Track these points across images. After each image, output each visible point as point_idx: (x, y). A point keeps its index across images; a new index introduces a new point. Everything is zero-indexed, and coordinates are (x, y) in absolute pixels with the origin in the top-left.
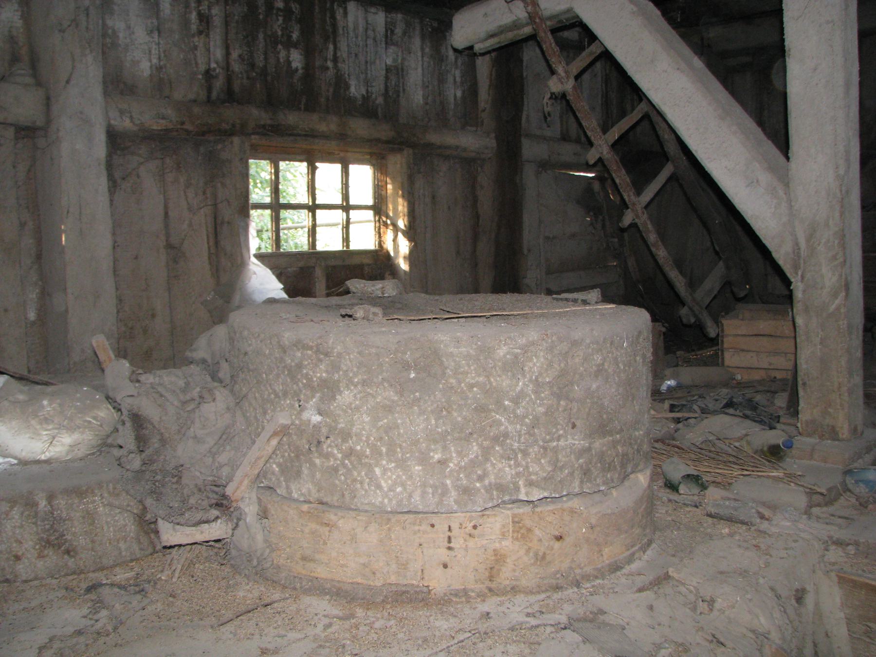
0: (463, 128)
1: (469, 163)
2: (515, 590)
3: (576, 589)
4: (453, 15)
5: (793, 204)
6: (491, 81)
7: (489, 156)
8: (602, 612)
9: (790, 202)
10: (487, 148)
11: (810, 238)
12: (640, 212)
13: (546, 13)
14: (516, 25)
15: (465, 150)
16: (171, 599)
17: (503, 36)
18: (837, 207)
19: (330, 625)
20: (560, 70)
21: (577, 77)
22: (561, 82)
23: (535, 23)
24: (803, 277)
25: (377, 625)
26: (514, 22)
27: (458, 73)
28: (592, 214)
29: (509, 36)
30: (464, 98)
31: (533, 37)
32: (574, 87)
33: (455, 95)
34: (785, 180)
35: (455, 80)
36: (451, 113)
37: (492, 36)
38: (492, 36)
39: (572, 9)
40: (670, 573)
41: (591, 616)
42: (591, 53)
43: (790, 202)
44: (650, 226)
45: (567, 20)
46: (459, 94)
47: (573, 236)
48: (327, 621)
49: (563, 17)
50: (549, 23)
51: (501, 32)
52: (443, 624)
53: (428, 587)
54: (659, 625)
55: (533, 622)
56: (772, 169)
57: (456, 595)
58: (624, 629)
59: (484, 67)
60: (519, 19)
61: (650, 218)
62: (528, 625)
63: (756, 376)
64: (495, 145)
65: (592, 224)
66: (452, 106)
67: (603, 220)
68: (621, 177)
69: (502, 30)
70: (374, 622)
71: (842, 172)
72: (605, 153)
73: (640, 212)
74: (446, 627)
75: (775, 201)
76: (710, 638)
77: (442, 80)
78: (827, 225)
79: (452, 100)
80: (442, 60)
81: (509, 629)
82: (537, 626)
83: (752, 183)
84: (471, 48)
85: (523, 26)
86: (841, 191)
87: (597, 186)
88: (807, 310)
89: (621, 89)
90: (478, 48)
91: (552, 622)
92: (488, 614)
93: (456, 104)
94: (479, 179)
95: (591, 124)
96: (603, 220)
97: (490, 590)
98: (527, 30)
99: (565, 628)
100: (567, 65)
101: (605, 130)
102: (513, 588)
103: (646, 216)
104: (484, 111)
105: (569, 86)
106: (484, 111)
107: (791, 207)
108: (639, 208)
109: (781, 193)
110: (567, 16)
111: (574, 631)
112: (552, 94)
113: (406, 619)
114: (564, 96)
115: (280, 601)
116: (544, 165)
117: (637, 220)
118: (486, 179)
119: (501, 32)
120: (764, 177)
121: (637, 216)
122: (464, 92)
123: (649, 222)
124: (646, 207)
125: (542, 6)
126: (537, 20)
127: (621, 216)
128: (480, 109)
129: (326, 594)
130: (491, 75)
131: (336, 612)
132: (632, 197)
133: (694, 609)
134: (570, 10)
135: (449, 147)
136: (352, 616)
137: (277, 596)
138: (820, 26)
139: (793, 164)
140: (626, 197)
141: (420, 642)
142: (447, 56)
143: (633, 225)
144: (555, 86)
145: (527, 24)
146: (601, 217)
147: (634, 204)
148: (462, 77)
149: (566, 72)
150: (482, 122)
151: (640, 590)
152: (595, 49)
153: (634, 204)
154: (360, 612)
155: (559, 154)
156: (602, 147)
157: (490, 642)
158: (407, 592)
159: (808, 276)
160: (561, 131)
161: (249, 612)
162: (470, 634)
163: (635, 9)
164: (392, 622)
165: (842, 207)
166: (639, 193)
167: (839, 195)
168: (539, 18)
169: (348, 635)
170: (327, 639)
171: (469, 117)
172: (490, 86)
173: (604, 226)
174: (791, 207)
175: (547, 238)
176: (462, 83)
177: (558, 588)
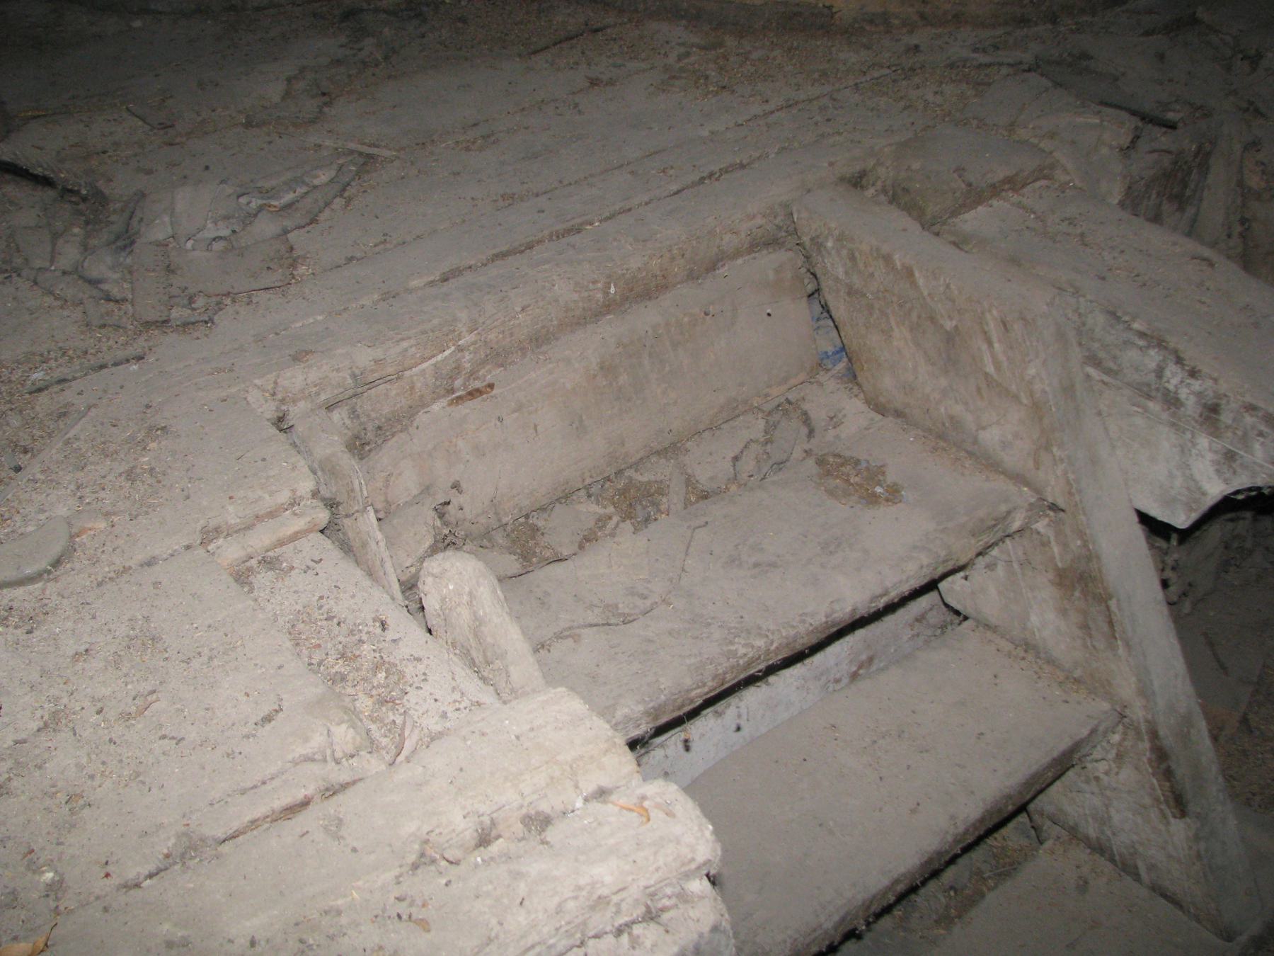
2: (958, 19)
3: (1050, 26)
8: (1089, 58)
16: (460, 25)
19: (688, 54)
25: (755, 55)
40: (1199, 15)
41: (1070, 60)
48: (682, 50)
52: (850, 57)
53: (830, 8)
54: (1170, 80)
55: (983, 59)
57: (871, 22)
58: (1116, 79)
62: (975, 63)
70: (750, 52)
74: (853, 60)
76: (1245, 105)
81: (946, 67)
82: (989, 65)
91: (1010, 61)
92: (917, 47)
97: (922, 16)
99: (1029, 70)
102: (956, 16)
111: (1042, 75)
113: (796, 49)
115: (615, 25)
129: (682, 17)
131: (696, 40)
133: (1229, 68)
136: (721, 44)
137: (610, 20)
141: (816, 76)
151: (1147, 33)
154: (730, 42)
157: (916, 80)
158: (800, 14)
161: (572, 38)
162: (887, 71)
164: (777, 52)
169: (712, 66)
170: (682, 70)
177: (1023, 21)
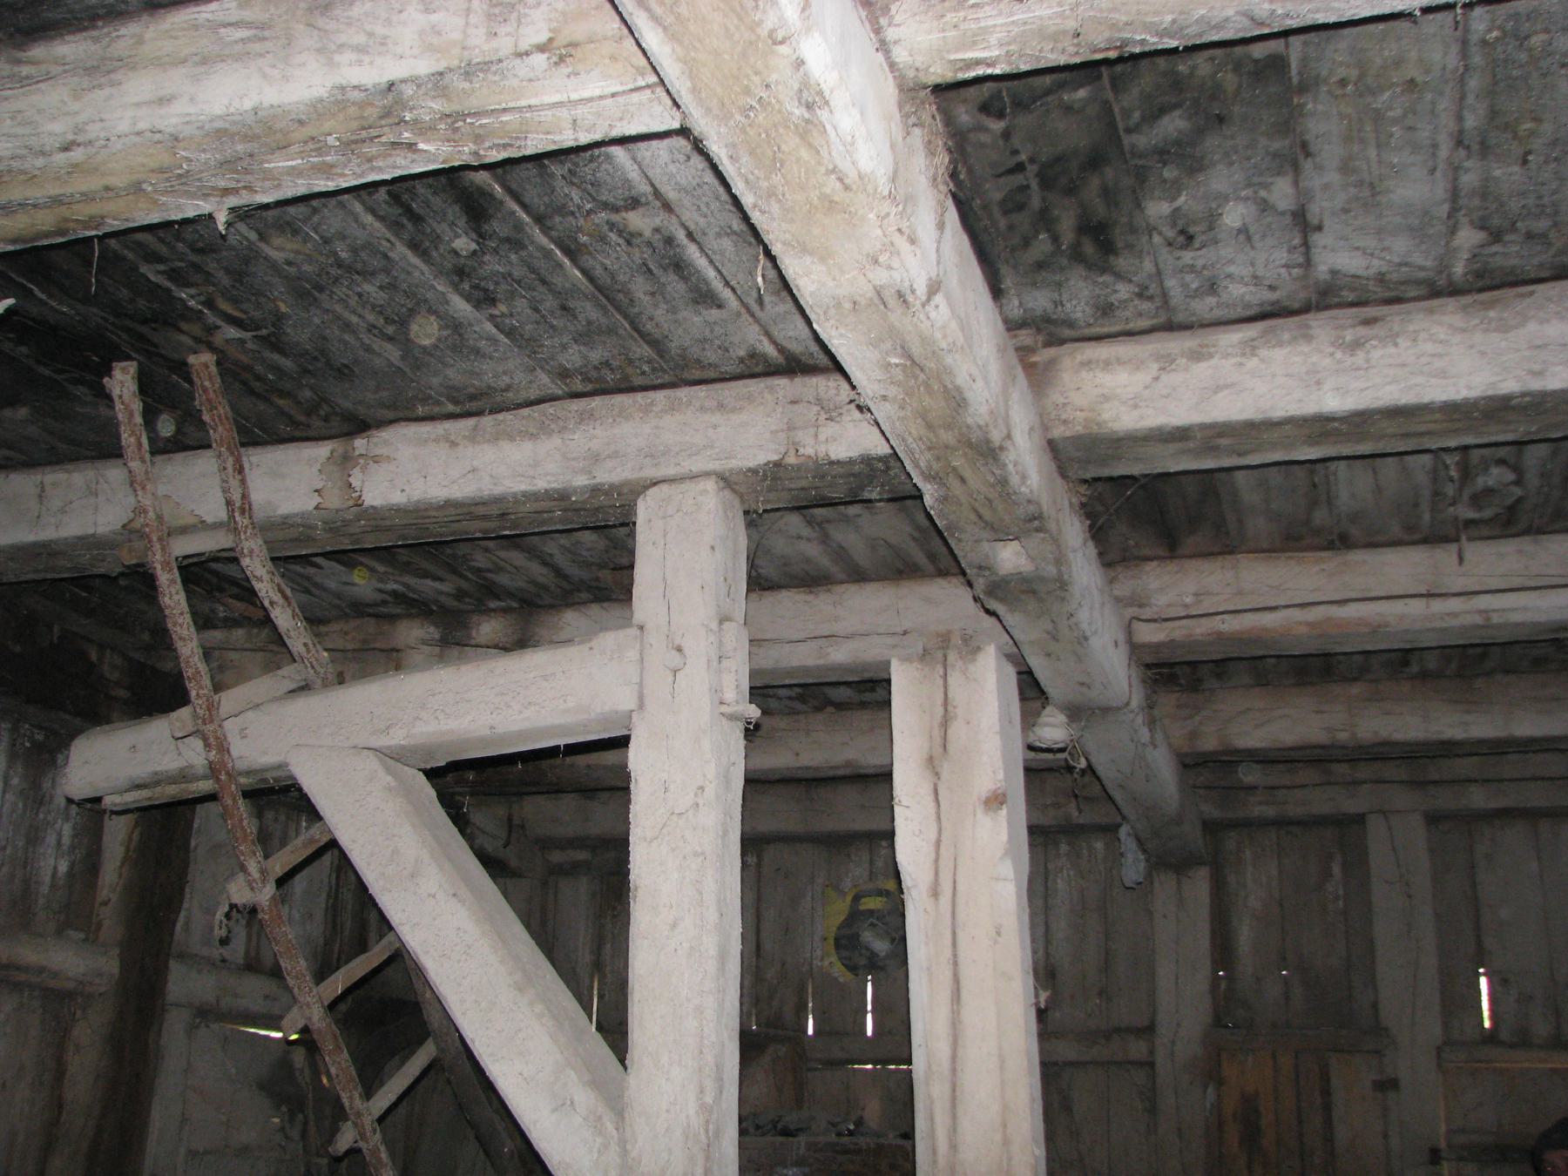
0: (59, 932)
1: (60, 1001)
4: (73, 735)
5: (629, 1147)
6: (128, 850)
7: (102, 990)
9: (623, 1142)
10: (100, 975)
12: (368, 1128)
13: (241, 765)
14: (184, 776)
15: (56, 975)
17: (158, 789)
18: (701, 1161)
20: (253, 867)
21: (281, 882)
22: (250, 885)
23: (218, 780)
26: (182, 769)
27: (67, 830)
28: (284, 1109)
29: (171, 792)
30: (71, 874)
31: (212, 797)
32: (273, 898)
33: (55, 868)
34: (617, 1104)
35: (59, 844)
36: (41, 901)
37: (138, 787)
38: (138, 787)
39: (287, 765)
42: (312, 841)
43: (623, 1142)
44: (384, 1155)
45: (275, 780)
46: (63, 867)
47: (244, 1150)
49: (268, 775)
50: (242, 780)
51: (157, 783)
56: (597, 1084)
59: (117, 835)
60: (191, 767)
61: (385, 1141)
64: (116, 971)
65: (282, 1129)
66: (45, 889)
67: (306, 1123)
68: (339, 1064)
69: (157, 781)
71: (709, 1099)
72: (316, 1018)
73: (368, 1128)
75: (599, 1140)
77: (34, 838)
79: (47, 879)
80: (41, 803)
83: (563, 1105)
84: (98, 800)
85: (198, 779)
86: (707, 1131)
87: (299, 1057)
89: (354, 914)
90: (109, 801)
93: (53, 886)
94: (75, 1033)
95: (297, 966)
96: (306, 1123)
98: (205, 786)
100: (266, 857)
101: (321, 975)
103: (378, 1136)
104: (105, 903)
105: (265, 894)
106: (105, 903)
107: (624, 1153)
108: (368, 1122)
109: (610, 1127)
110: (276, 774)
112: (233, 906)
114: (253, 911)
116: (205, 1013)
117: (361, 1144)
118: (89, 1035)
119: (157, 783)
120: (584, 1098)
121: (363, 1136)
122: (72, 865)
123: (383, 1148)
124: (381, 1120)
125: (235, 752)
126: (223, 777)
127: (334, 1131)
128: (99, 900)
130: (130, 839)
132: (358, 1102)
134: (282, 766)
135: (26, 969)
139: (633, 1080)
140: (346, 1101)
142: (52, 797)
143: (354, 1152)
144: (239, 892)
145: (205, 777)
146: (300, 1116)
147: (359, 1114)
148: (75, 836)
149: (263, 872)
150: (99, 925)
152: (317, 835)
153: (359, 1114)
155: (236, 995)
156: (311, 1005)
160: (247, 952)
163: (393, 784)
165: (708, 1159)
166: (368, 1094)
167: (703, 1137)
168: (228, 774)
171: (75, 912)
172: (126, 858)
173: (304, 1135)
174: (624, 1153)
175: (193, 1153)
176: (73, 848)
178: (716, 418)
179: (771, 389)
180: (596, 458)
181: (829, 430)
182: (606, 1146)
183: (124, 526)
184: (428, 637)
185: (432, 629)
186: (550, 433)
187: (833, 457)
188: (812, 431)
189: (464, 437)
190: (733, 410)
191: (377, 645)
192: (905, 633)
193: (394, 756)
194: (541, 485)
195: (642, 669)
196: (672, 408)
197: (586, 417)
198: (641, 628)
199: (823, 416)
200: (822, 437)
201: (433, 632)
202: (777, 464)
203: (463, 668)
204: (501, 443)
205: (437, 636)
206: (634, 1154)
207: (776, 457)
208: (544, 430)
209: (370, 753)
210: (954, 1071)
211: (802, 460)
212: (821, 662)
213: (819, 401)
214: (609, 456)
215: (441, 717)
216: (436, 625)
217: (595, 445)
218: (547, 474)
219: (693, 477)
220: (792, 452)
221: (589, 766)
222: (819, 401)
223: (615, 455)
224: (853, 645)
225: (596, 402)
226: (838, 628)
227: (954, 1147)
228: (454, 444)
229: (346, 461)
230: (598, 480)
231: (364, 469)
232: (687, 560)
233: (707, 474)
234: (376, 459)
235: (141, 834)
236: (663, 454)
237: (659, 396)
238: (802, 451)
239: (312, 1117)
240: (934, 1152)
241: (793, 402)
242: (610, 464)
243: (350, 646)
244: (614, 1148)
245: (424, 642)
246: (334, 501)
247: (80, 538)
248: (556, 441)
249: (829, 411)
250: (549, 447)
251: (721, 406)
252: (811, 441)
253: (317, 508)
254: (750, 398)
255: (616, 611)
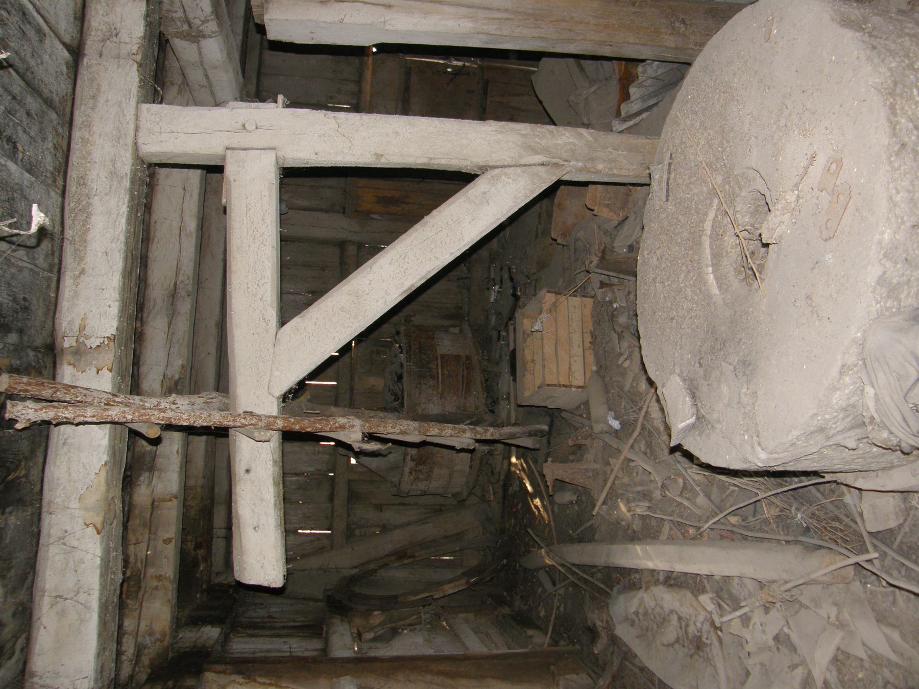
6: (270, 684)
11: (536, 152)
24: (566, 161)
63: (591, 358)
78: (525, 136)
83: (485, 198)
88: (592, 159)
130: (264, 684)
138: (362, 125)
159: (565, 155)
178: (102, 100)
179: (89, 67)
180: (113, 174)
181: (124, 36)
182: (506, 174)
183: (99, 533)
184: (146, 482)
185: (142, 478)
186: (89, 204)
187: (142, 34)
188: (122, 46)
189: (79, 264)
190: (98, 90)
191: (148, 516)
192: (184, 189)
193: (282, 322)
194: (124, 209)
195: (253, 149)
196: (88, 125)
197: (82, 181)
198: (228, 149)
199: (115, 39)
200: (128, 40)
201: (144, 477)
202: (140, 65)
203: (234, 268)
204: (88, 238)
205: (147, 474)
206: (509, 160)
207: (136, 66)
208: (86, 212)
209: (279, 334)
210: (472, 7)
211: (140, 52)
212: (194, 235)
213: (104, 40)
214: (113, 166)
215: (262, 282)
216: (140, 476)
217: (104, 174)
218: (118, 206)
219: (137, 117)
220: (134, 57)
221: (204, 477)
222: (104, 40)
223: (113, 162)
224: (187, 218)
225: (73, 174)
226: (176, 225)
227: (506, 10)
228: (83, 272)
229: (79, 352)
230: (129, 172)
231: (88, 337)
232: (184, 131)
233: (137, 107)
234: (82, 328)
235: (261, 676)
236: (119, 131)
237: (77, 134)
238: (134, 51)
239: (401, 623)
240: (508, 19)
241: (101, 56)
242: (118, 165)
243: (147, 536)
244: (507, 170)
245: (150, 483)
246: (109, 357)
247: (102, 575)
248: (95, 201)
249: (111, 36)
250: (98, 206)
251: (94, 97)
252: (128, 47)
253: (110, 371)
254: (92, 80)
255: (238, 95)
